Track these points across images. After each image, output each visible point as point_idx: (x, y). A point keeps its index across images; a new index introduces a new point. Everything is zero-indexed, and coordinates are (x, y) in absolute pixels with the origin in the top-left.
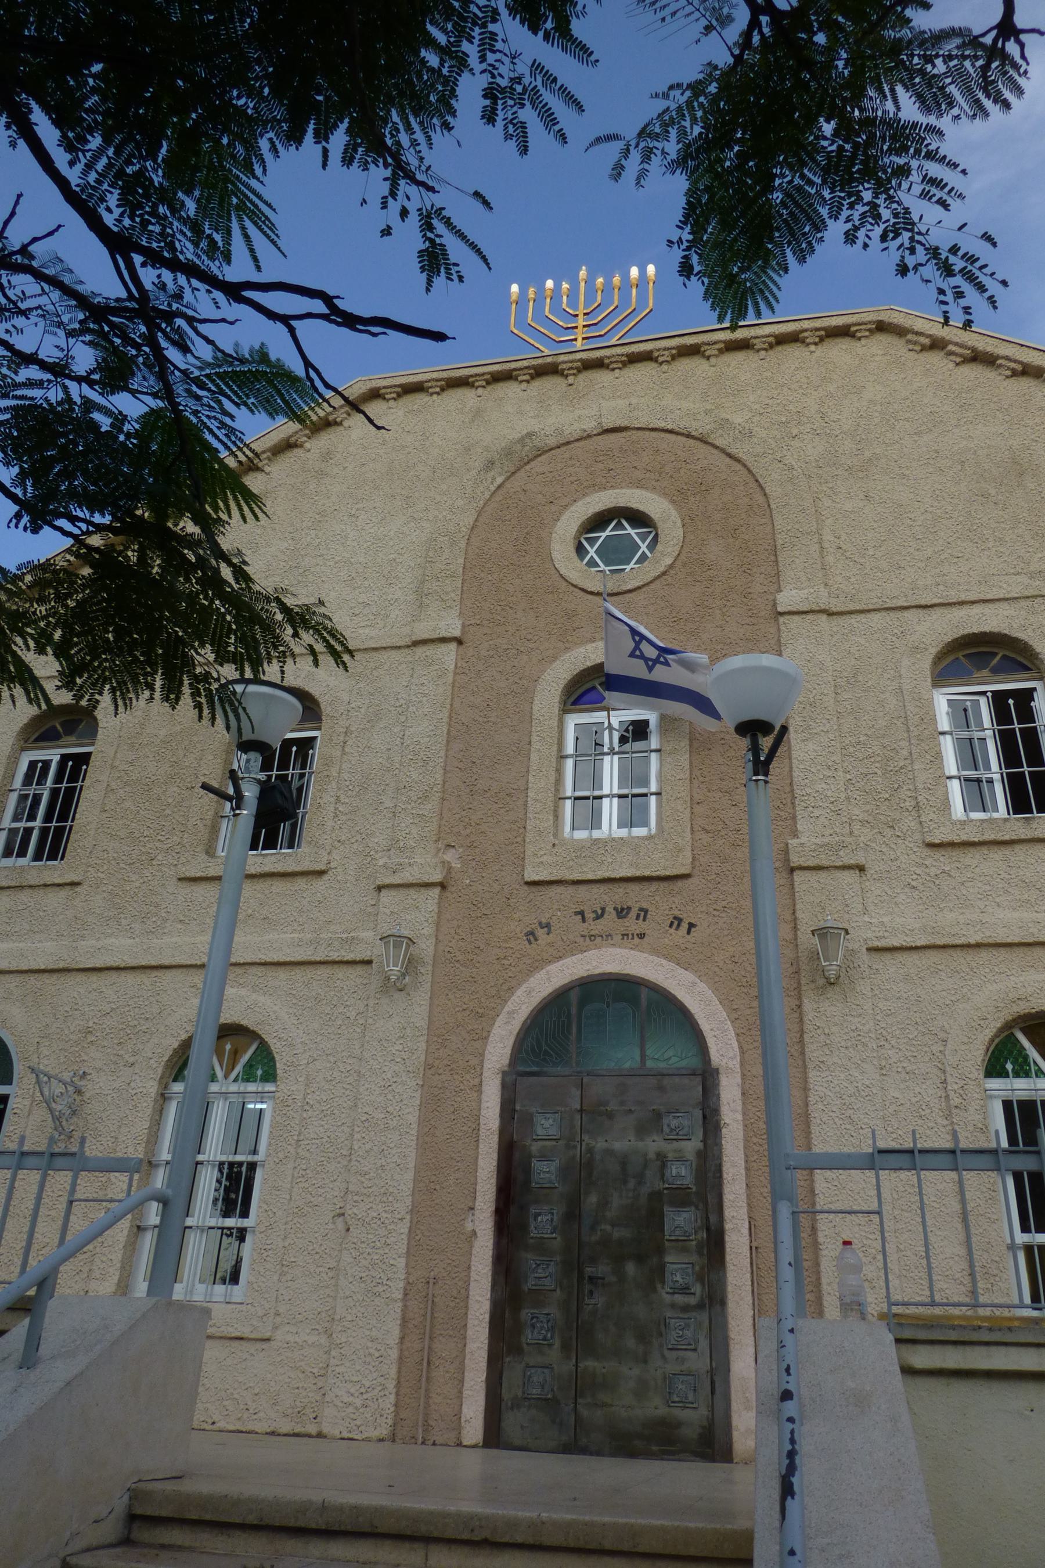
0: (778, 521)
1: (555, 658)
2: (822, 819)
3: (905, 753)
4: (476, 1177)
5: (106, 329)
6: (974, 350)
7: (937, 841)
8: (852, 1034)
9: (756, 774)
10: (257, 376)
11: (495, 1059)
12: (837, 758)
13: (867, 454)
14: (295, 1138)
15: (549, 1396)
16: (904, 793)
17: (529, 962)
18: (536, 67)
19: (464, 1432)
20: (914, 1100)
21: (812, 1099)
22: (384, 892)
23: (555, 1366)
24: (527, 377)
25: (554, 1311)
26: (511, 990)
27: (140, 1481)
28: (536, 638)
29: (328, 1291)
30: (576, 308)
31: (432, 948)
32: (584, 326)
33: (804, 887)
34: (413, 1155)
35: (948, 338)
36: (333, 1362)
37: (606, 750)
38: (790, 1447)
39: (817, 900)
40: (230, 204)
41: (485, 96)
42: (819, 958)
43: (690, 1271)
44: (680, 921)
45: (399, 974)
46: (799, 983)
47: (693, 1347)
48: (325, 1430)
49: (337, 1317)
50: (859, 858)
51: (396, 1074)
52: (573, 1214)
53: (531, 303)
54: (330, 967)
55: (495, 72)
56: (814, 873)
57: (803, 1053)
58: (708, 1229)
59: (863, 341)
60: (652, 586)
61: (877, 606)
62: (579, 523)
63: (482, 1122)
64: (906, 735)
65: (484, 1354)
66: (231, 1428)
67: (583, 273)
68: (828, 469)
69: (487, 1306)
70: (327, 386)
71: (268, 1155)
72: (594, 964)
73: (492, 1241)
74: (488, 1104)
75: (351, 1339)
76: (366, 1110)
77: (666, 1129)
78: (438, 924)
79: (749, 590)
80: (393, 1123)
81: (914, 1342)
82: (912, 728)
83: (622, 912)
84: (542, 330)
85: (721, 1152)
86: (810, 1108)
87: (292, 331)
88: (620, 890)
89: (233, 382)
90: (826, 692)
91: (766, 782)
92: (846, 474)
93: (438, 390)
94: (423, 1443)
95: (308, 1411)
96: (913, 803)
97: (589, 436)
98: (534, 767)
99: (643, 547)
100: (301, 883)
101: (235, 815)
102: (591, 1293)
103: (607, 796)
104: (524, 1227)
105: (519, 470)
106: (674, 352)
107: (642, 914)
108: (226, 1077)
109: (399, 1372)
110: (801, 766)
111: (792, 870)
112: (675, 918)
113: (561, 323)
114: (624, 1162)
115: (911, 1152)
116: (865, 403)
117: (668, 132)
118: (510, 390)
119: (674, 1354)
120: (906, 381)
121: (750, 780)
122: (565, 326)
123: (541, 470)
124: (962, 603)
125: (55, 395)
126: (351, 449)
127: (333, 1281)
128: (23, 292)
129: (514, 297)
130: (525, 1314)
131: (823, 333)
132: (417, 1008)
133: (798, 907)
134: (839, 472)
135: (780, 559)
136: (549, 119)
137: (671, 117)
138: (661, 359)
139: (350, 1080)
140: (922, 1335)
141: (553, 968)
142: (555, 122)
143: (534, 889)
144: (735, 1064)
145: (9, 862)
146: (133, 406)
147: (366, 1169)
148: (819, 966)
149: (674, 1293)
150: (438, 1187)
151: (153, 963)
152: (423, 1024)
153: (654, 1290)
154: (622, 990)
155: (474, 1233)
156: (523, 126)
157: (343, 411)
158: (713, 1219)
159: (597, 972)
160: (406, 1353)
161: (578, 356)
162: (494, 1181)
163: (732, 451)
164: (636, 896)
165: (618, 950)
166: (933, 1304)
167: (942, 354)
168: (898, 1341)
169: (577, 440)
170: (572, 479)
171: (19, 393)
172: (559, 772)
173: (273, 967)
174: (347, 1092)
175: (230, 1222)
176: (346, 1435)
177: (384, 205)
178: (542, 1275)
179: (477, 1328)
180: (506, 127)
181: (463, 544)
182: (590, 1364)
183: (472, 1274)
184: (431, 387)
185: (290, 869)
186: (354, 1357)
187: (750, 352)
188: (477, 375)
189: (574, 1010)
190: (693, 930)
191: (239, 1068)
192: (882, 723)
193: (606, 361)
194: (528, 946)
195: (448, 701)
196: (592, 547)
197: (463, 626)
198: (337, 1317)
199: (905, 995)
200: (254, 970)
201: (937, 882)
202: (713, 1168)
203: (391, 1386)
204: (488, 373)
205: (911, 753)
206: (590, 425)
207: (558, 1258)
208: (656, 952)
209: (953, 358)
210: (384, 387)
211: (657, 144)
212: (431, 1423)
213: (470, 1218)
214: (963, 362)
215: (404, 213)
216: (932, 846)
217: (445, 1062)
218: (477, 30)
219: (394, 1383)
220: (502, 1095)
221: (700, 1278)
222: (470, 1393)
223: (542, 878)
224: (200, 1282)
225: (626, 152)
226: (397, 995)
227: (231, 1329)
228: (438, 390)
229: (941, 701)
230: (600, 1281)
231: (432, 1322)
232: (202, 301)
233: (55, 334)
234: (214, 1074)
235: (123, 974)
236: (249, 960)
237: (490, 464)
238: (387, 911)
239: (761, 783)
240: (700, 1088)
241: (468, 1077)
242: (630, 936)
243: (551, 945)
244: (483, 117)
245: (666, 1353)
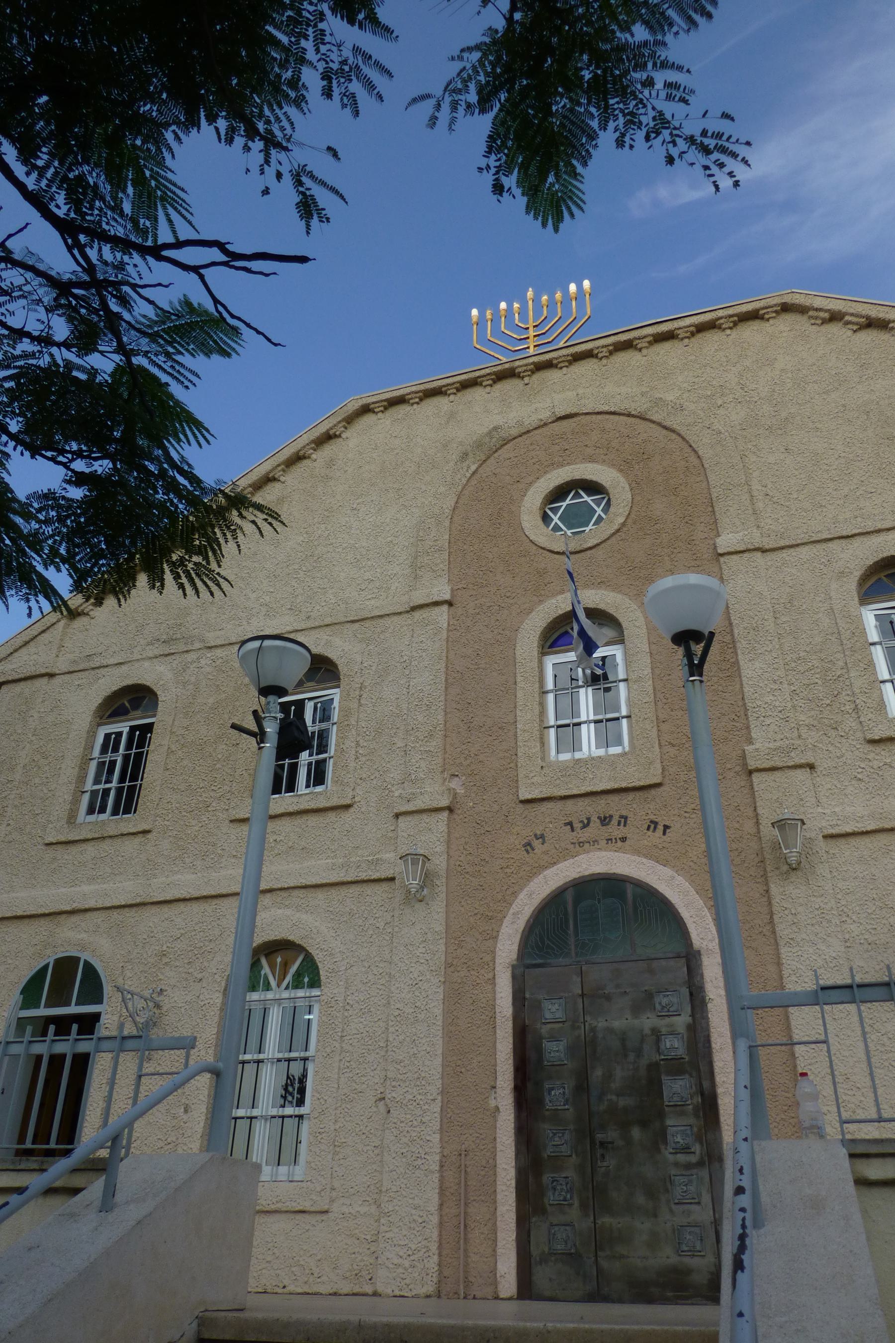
0: (712, 477)
1: (531, 610)
2: (773, 727)
3: (841, 663)
4: (496, 1059)
5: (74, 302)
6: (868, 318)
7: (877, 738)
8: (816, 912)
9: (692, 675)
10: (191, 326)
11: (504, 955)
12: (782, 673)
13: (784, 415)
14: (340, 1034)
15: (573, 1251)
16: (843, 698)
17: (528, 869)
18: (356, 50)
19: (500, 1287)
20: (877, 968)
21: (785, 973)
22: (401, 819)
24: (490, 382)
25: (571, 1173)
26: (515, 894)
27: (206, 1311)
28: (514, 595)
29: (375, 1167)
30: (527, 322)
31: (445, 863)
32: (535, 336)
33: (762, 786)
34: (441, 1042)
35: (844, 310)
36: (383, 1228)
37: (580, 683)
38: (742, 1231)
39: (774, 796)
40: (156, 197)
41: (323, 79)
42: (780, 848)
43: (689, 1132)
44: (656, 823)
45: (418, 887)
46: (765, 870)
47: (696, 1201)
48: (380, 1288)
49: (384, 1189)
50: (809, 758)
51: (421, 973)
52: (582, 1087)
53: (489, 323)
54: (360, 886)
55: (328, 59)
56: (770, 773)
57: (774, 932)
58: (702, 1095)
59: (771, 321)
60: (609, 542)
61: (805, 541)
62: (543, 496)
63: (497, 1011)
64: (840, 648)
65: (513, 1216)
66: (300, 1290)
67: (530, 294)
68: (751, 430)
69: (512, 1173)
70: (233, 316)
71: (318, 1051)
72: (584, 866)
73: (513, 1115)
75: (397, 1208)
76: (398, 1006)
77: (658, 1006)
78: (448, 842)
79: (692, 538)
80: (421, 1017)
81: (867, 1156)
82: (845, 642)
83: (605, 820)
84: (500, 343)
85: (708, 1025)
86: (784, 980)
87: (202, 277)
88: (602, 801)
89: (176, 334)
90: (766, 617)
91: (701, 682)
92: (767, 432)
93: (417, 400)
94: (465, 1298)
95: (364, 1273)
96: (853, 706)
97: (545, 424)
98: (520, 703)
99: (599, 511)
100: (332, 816)
101: (260, 748)
102: (603, 1156)
103: (585, 722)
104: (540, 1102)
105: (489, 458)
106: (611, 348)
107: (623, 820)
108: (279, 986)
109: (440, 1235)
110: (750, 683)
111: (750, 773)
112: (652, 822)
113: (515, 336)
114: (623, 1038)
115: (849, 987)
116: (778, 373)
117: (468, 86)
118: (477, 394)
119: (681, 1208)
120: (811, 350)
121: (688, 681)
122: (519, 337)
123: (507, 456)
124: (879, 531)
125: (44, 361)
126: (350, 456)
127: (379, 1157)
128: (12, 283)
129: (475, 319)
130: (546, 1178)
131: (736, 318)
132: (434, 916)
133: (758, 804)
134: (761, 431)
135: (716, 509)
136: (370, 86)
137: (469, 75)
138: (600, 355)
139: (383, 981)
140: (874, 1150)
142: (373, 87)
143: (528, 806)
144: (715, 945)
145: (92, 818)
146: (103, 363)
147: (401, 1058)
148: (780, 856)
149: (676, 1153)
150: (463, 1070)
151: (213, 893)
152: (440, 927)
153: (659, 1151)
154: (612, 885)
156: (353, 95)
157: (341, 425)
158: (706, 1084)
159: (587, 873)
160: (445, 1218)
161: (531, 360)
162: (511, 1061)
163: (668, 423)
164: (615, 806)
165: (604, 853)
166: (880, 1120)
167: (840, 324)
168: (852, 1156)
169: (536, 429)
170: (533, 461)
171: (17, 364)
172: (542, 705)
173: (313, 890)
174: (381, 992)
175: (289, 1111)
176: (398, 1293)
177: (262, 172)
180: (342, 99)
181: (447, 523)
182: (606, 1220)
183: (498, 1145)
184: (412, 399)
185: (321, 806)
186: (401, 1224)
187: (676, 342)
188: (448, 385)
189: (570, 908)
190: (668, 831)
191: (289, 978)
192: (818, 639)
193: (555, 362)
194: (526, 855)
195: (444, 654)
196: (555, 515)
197: (452, 590)
198: (384, 1189)
199: (861, 875)
200: (296, 893)
201: (881, 773)
202: (702, 1039)
203: (434, 1247)
204: (457, 382)
205: (846, 663)
206: (545, 415)
207: (572, 1127)
208: (637, 852)
209: (850, 326)
211: (460, 97)
212: (470, 1279)
214: (860, 329)
215: (279, 176)
217: (463, 960)
218: (311, 30)
219: (437, 1245)
220: (513, 986)
221: (699, 1138)
222: (504, 1251)
223: (534, 796)
224: (267, 1165)
225: (438, 107)
226: (418, 905)
227: (294, 1204)
228: (417, 400)
229: (869, 617)
230: (610, 1146)
231: (466, 1190)
232: (141, 269)
233: (36, 311)
234: (269, 983)
235: (189, 904)
236: (292, 885)
237: (465, 456)
238: (405, 834)
239: (697, 683)
240: (685, 969)
241: (482, 972)
242: (614, 841)
243: (546, 853)
244: (323, 94)
245: (674, 1207)
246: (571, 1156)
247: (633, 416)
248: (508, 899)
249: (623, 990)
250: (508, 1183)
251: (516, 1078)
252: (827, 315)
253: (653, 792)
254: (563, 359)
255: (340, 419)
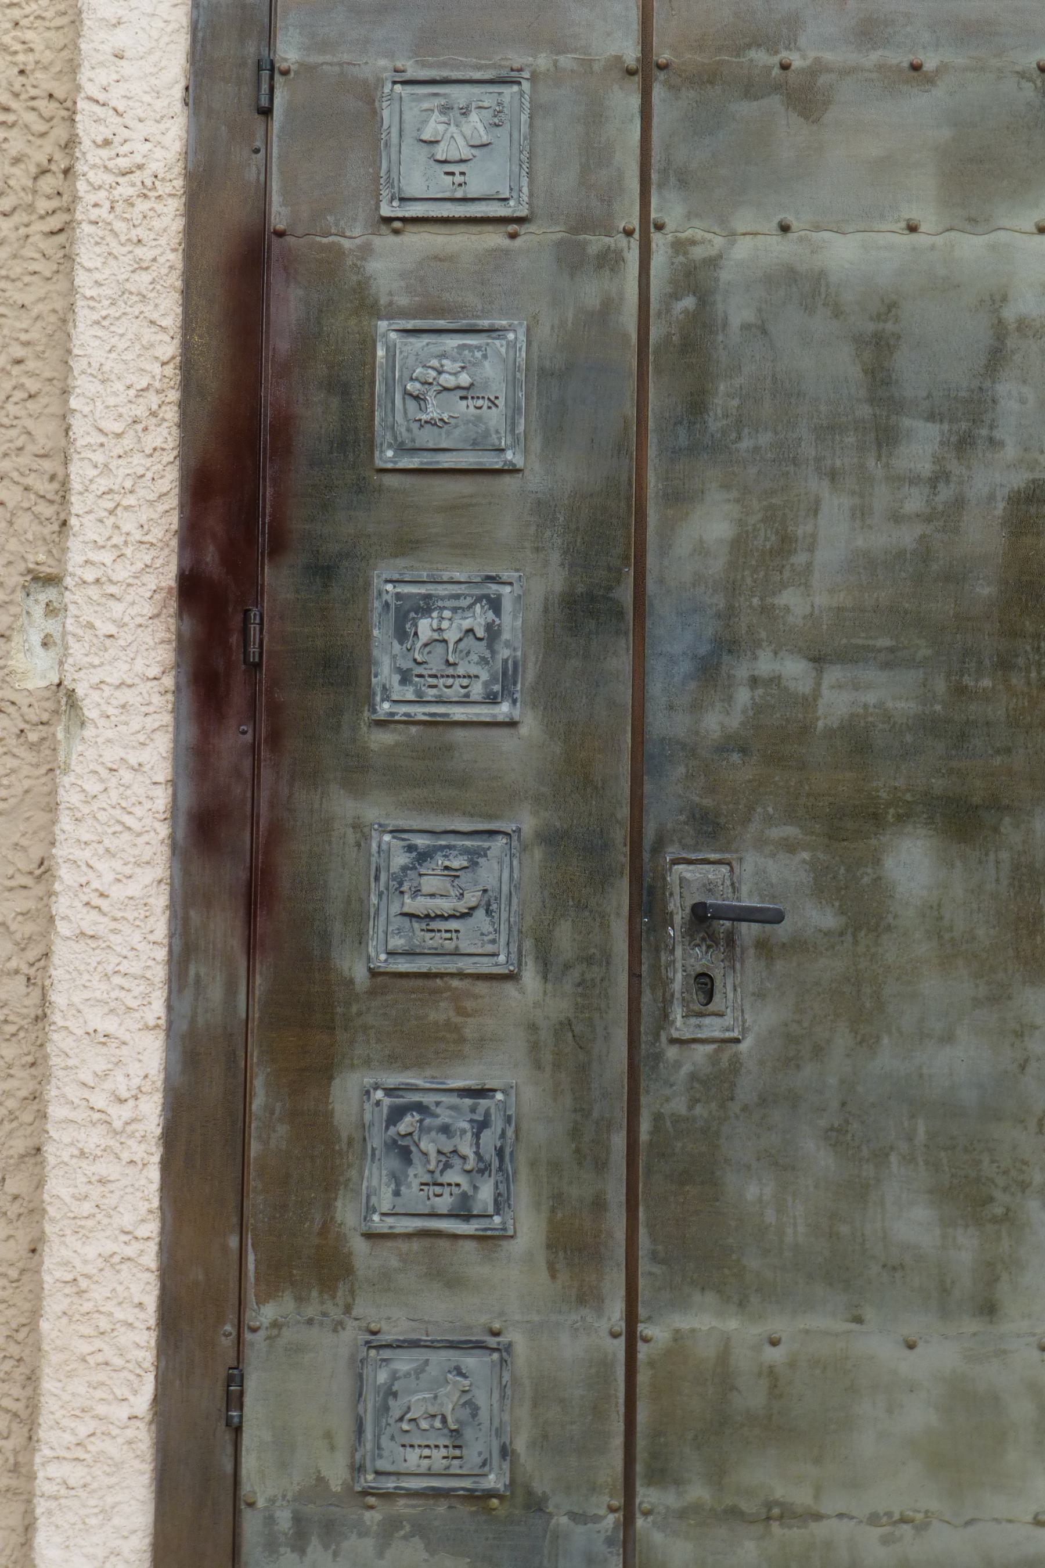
4: (64, 418)
15: (492, 1481)
23: (515, 1337)
25: (505, 1070)
52: (602, 599)
63: (88, 130)
73: (163, 743)
74: (121, 38)
102: (705, 985)
104: (342, 671)
130: (356, 1094)
155: (65, 701)
162: (164, 436)
178: (445, 905)
179: (102, 1168)
182: (697, 1324)
183: (61, 906)
207: (527, 822)
213: (39, 625)
222: (76, 1474)
230: (748, 931)
246: (511, 977)
249: (902, 58)
250: (120, 1114)
251: (192, 534)
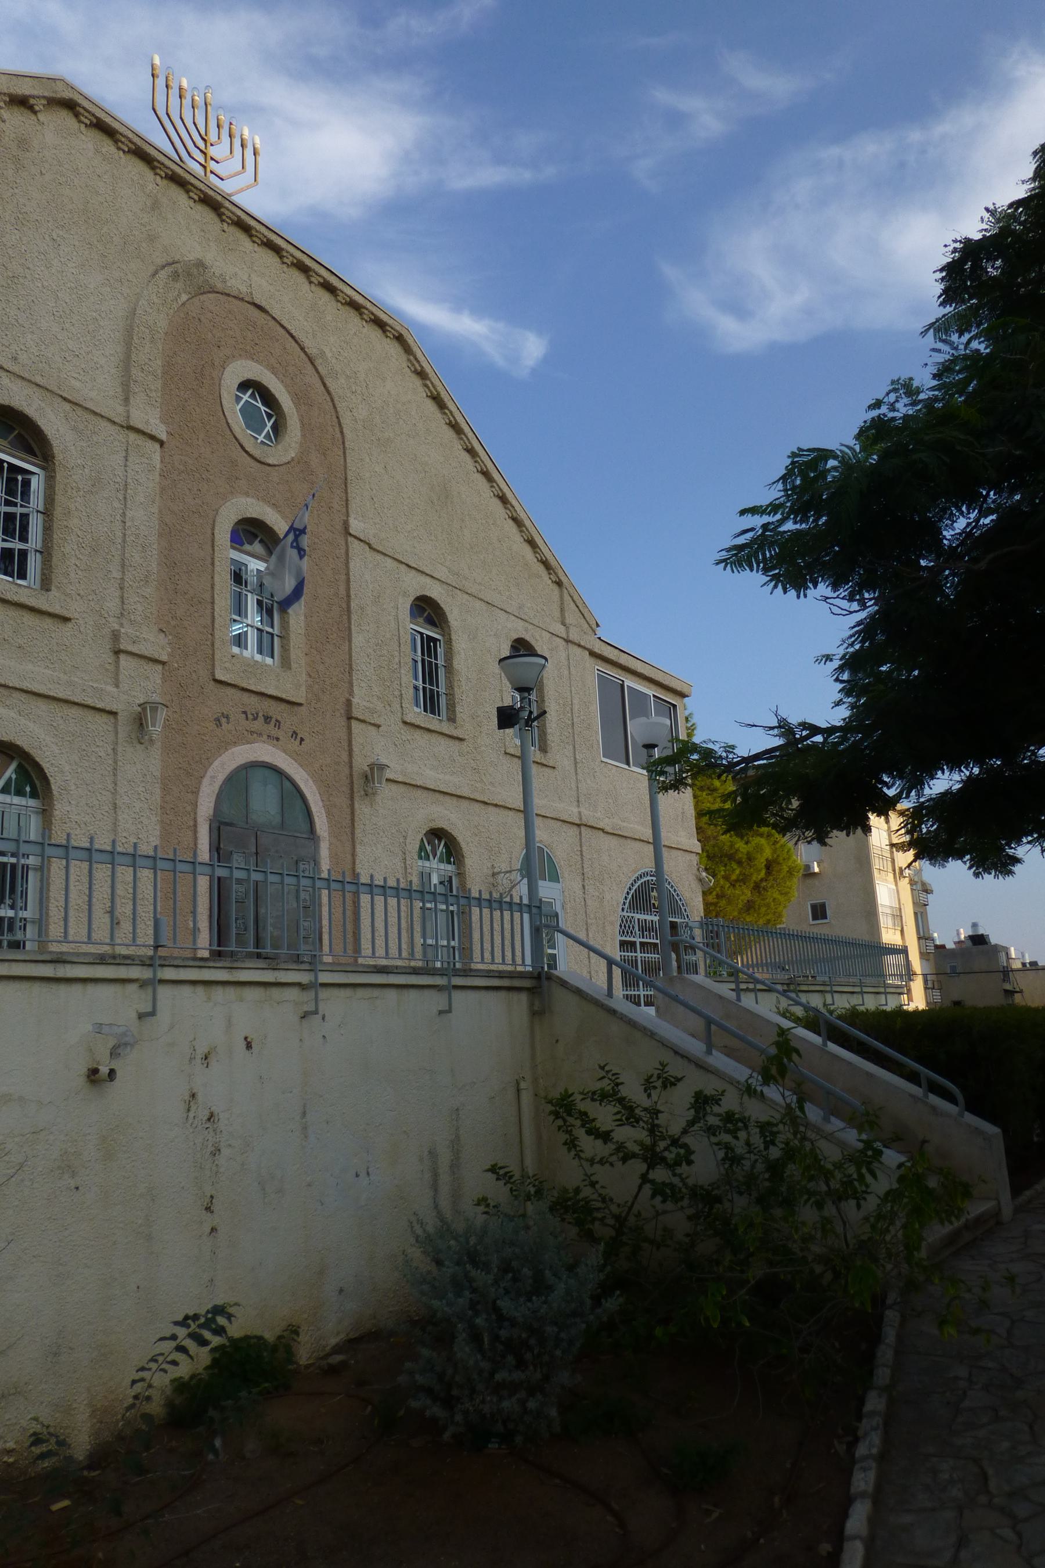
6: (439, 394)
76: (125, 834)
88: (267, 703)
93: (126, 149)
100: (48, 622)
138: (285, 260)
141: (237, 749)
143: (218, 686)
144: (326, 835)
187: (333, 298)
200: (16, 695)
210: (84, 108)
216: (405, 723)
228: (126, 149)
243: (229, 732)
247: (305, 352)
248: (206, 763)
252: (419, 368)
253: (296, 708)
254: (261, 236)
255: (46, 94)
